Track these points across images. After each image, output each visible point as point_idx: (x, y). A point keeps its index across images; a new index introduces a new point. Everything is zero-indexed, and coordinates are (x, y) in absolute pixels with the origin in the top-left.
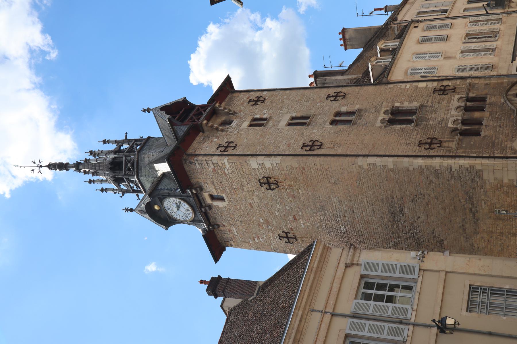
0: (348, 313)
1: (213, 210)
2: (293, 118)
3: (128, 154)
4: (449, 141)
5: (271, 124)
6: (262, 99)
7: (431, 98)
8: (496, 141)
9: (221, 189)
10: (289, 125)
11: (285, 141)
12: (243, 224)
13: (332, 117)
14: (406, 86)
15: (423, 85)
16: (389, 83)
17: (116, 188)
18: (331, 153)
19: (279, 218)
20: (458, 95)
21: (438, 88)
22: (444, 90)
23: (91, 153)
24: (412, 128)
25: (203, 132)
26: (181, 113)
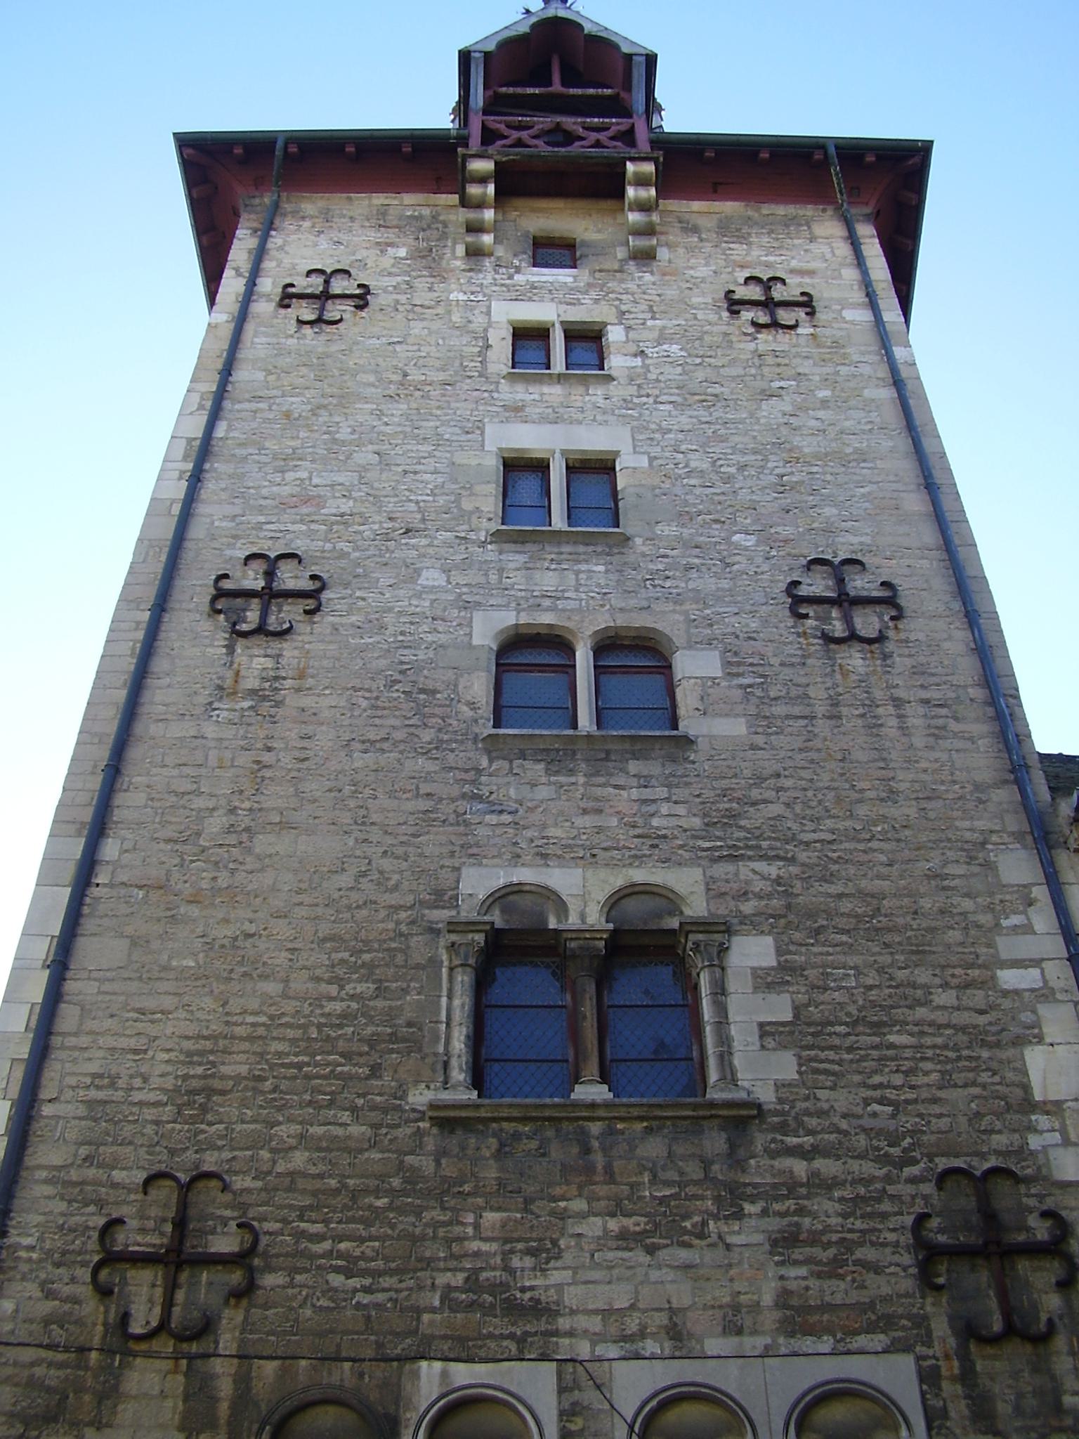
7: (869, 1168)
20: (929, 1377)
21: (1004, 1197)
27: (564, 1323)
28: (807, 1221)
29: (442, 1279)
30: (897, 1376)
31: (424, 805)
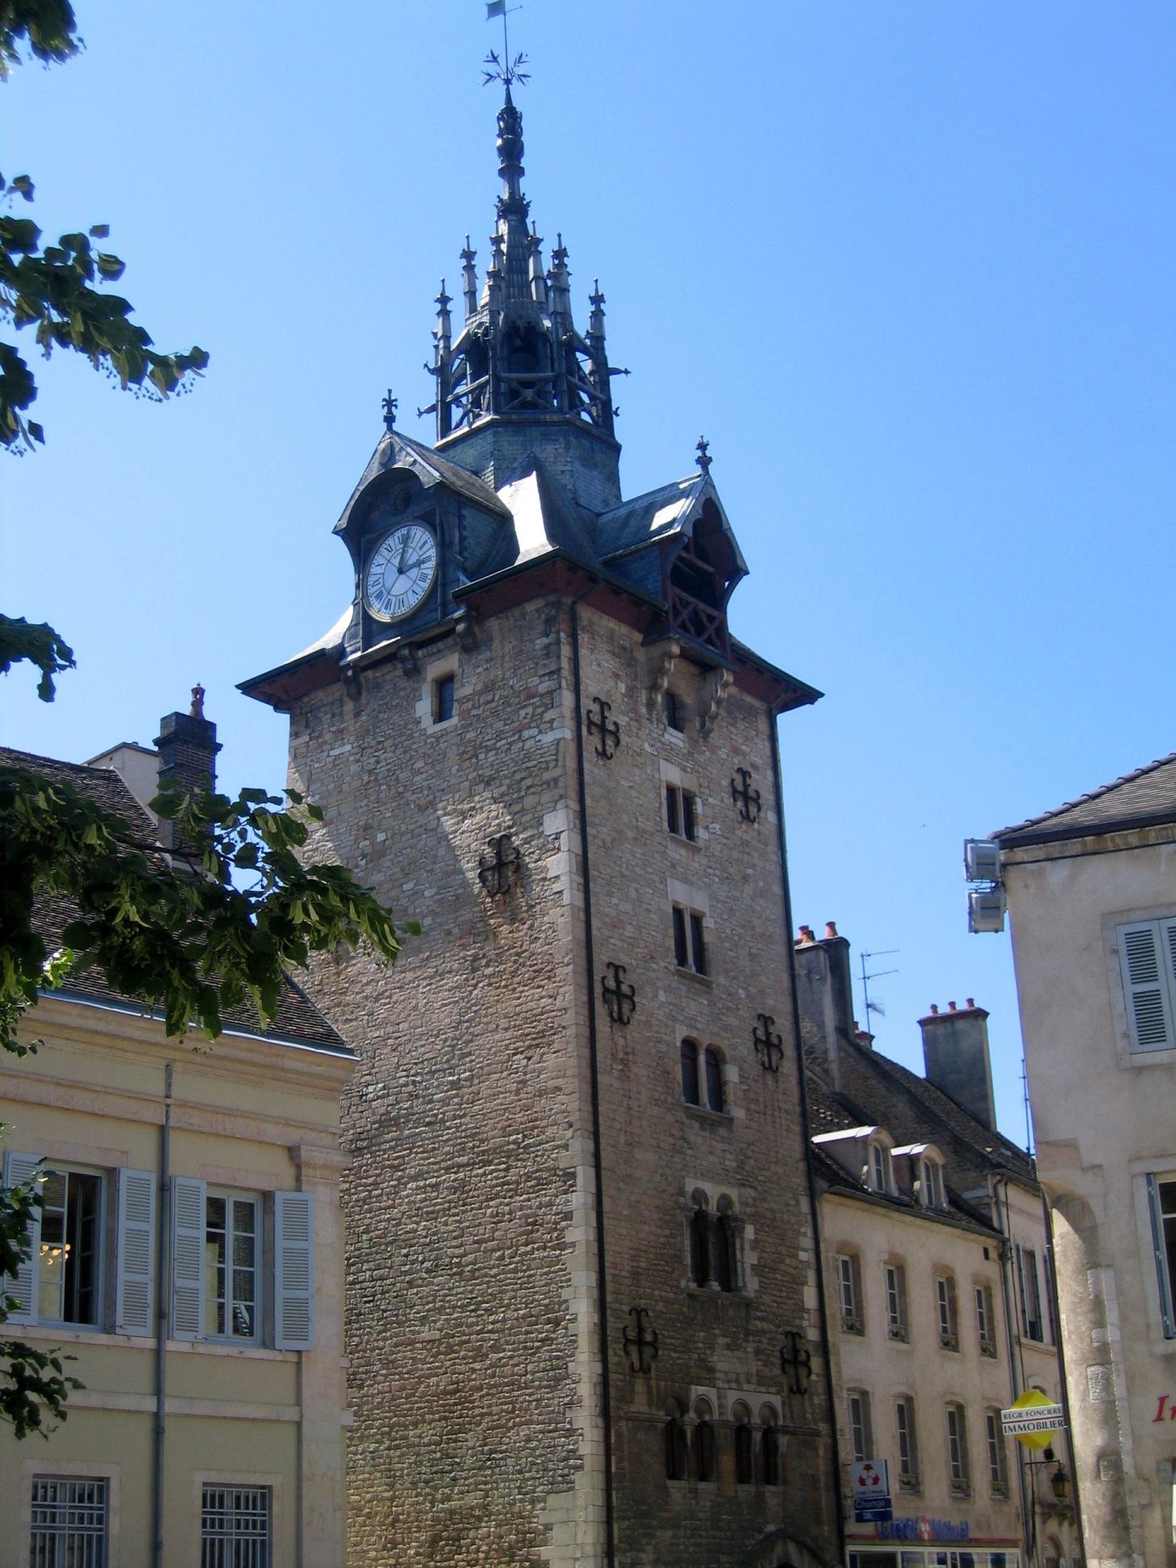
0: (172, 1170)
1: (404, 683)
2: (697, 920)
3: (565, 387)
4: (650, 1392)
5: (678, 853)
6: (753, 810)
7: (773, 1328)
8: (654, 1523)
9: (475, 712)
10: (678, 913)
11: (625, 907)
12: (366, 777)
13: (705, 1041)
14: (805, 1250)
16: (813, 1196)
17: (454, 346)
18: (600, 1056)
19: (393, 893)
20: (783, 1403)
21: (801, 1344)
23: (560, 254)
24: (683, 1284)
25: (643, 644)
26: (700, 563)
27: (718, 1375)
30: (776, 1401)
31: (671, 1140)
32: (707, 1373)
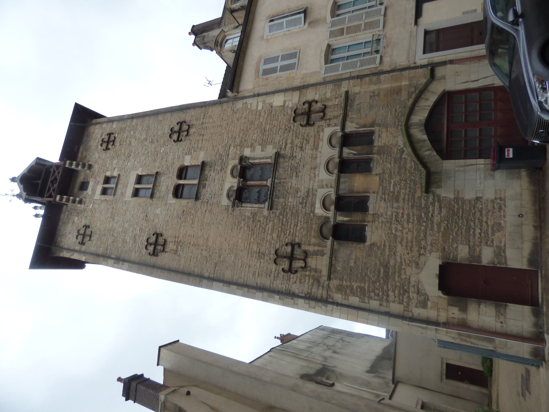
7: (291, 134)
8: (392, 262)
15: (278, 100)
18: (174, 265)
20: (329, 125)
21: (299, 112)
22: (308, 113)
27: (311, 187)
28: (298, 145)
29: (300, 208)
31: (207, 211)
32: (310, 193)
